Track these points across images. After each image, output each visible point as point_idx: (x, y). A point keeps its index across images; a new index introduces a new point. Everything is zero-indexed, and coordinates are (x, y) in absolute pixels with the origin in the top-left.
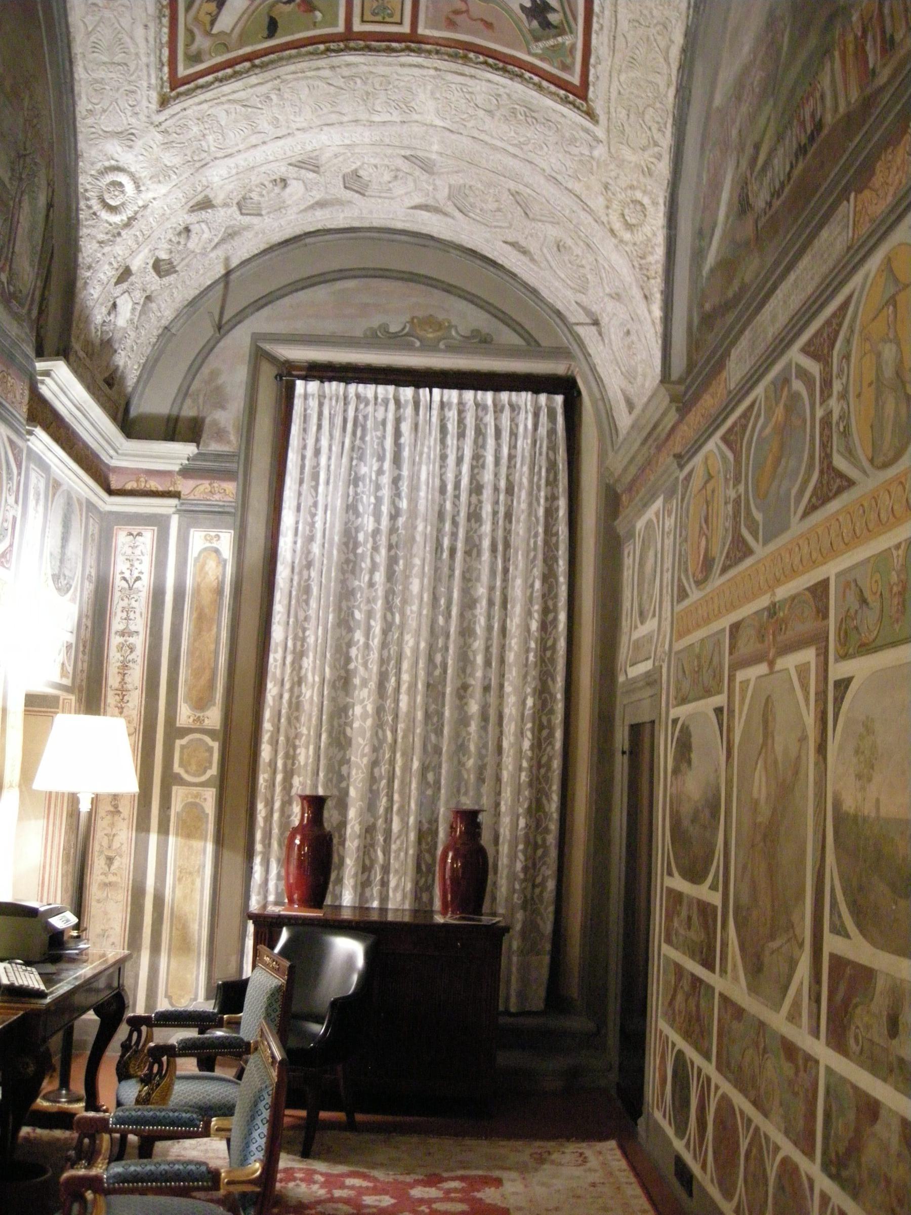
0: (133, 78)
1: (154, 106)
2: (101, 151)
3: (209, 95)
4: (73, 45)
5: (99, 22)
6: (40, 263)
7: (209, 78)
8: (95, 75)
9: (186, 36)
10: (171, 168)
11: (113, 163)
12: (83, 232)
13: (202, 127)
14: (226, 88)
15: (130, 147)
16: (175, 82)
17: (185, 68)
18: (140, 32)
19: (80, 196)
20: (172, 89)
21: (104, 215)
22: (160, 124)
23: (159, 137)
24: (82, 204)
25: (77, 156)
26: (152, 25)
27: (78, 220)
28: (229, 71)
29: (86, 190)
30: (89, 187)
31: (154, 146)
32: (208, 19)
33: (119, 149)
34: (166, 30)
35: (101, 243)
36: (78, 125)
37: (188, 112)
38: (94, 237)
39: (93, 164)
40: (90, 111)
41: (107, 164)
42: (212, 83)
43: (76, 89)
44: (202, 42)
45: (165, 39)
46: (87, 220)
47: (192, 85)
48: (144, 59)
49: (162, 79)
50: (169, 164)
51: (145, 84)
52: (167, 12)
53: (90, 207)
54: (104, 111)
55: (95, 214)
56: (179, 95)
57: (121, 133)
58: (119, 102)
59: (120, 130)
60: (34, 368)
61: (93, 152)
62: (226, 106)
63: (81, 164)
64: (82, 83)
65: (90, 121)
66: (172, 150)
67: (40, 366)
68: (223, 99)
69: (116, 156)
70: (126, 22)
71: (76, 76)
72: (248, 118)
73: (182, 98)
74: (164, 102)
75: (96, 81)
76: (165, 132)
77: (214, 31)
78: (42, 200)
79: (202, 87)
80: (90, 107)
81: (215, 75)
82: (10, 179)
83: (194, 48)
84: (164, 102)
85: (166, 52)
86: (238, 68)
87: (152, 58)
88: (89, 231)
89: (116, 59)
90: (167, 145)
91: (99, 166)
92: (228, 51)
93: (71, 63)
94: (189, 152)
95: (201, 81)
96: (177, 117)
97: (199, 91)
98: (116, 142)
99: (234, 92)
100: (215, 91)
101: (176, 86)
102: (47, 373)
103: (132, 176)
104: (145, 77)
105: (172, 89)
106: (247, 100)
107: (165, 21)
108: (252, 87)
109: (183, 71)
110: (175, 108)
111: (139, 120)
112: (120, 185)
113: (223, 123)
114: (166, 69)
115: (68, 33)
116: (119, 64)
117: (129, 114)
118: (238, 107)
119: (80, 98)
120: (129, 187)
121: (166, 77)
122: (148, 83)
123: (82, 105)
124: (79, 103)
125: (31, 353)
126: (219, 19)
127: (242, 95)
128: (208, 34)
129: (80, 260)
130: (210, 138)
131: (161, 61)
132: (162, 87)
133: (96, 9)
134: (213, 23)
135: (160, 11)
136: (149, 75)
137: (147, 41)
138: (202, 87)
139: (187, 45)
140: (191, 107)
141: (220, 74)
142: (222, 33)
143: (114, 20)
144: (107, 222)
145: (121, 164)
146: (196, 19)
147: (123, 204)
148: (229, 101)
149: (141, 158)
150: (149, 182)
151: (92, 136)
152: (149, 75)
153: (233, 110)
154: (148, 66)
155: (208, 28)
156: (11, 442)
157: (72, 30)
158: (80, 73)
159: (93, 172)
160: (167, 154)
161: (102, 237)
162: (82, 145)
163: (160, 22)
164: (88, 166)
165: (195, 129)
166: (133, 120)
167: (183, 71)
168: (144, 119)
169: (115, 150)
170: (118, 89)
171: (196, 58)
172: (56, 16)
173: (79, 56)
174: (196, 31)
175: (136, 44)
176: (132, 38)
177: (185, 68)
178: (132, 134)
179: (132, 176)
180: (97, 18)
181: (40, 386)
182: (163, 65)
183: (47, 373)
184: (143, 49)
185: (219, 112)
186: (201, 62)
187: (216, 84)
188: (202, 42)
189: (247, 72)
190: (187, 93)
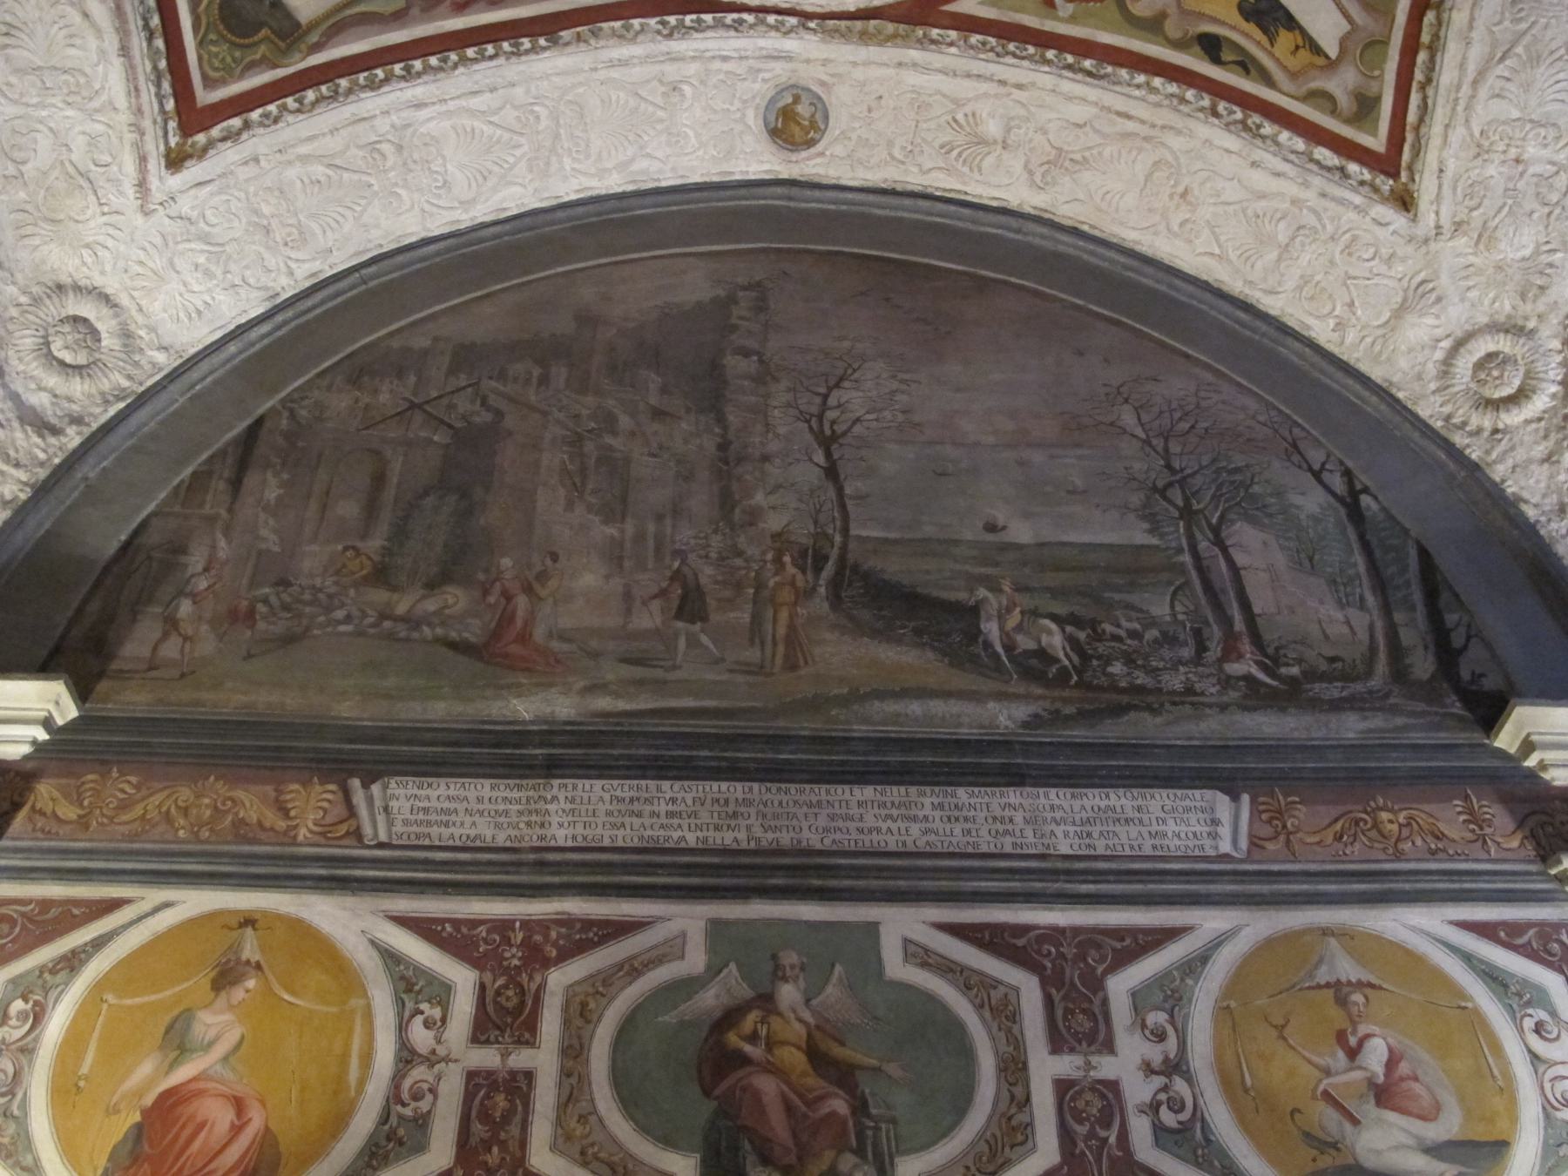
0: (1330, 228)
1: (1399, 220)
2: (1410, 350)
3: (1440, 115)
4: (1225, 288)
5: (1213, 233)
6: (1381, 585)
7: (1415, 99)
8: (1290, 284)
9: (1316, 107)
10: (1537, 252)
11: (1446, 344)
12: (1498, 472)
13: (1497, 158)
14: (1447, 76)
15: (1439, 300)
16: (1387, 163)
17: (1374, 133)
18: (1259, 179)
19: (1444, 432)
20: (1395, 175)
21: (1512, 418)
22: (1438, 227)
23: (1462, 242)
24: (1459, 439)
25: (1383, 393)
26: (1259, 154)
27: (1475, 468)
28: (1422, 57)
29: (1448, 418)
30: (1447, 409)
31: (1472, 259)
32: (1304, 55)
33: (1430, 321)
34: (1285, 136)
35: (1547, 459)
36: (1345, 358)
37: (1452, 166)
38: (1530, 461)
39: (1419, 377)
40: (1340, 326)
41: (1439, 355)
42: (1425, 99)
43: (1291, 323)
44: (1341, 84)
45: (1300, 144)
46: (1488, 452)
47: (1410, 137)
48: (1310, 196)
49: (1362, 183)
50: (1527, 252)
51: (1352, 215)
52: (1256, 118)
53: (1478, 432)
54: (1351, 304)
55: (1496, 431)
56: (1410, 168)
57: (1405, 300)
58: (1352, 272)
59: (1399, 300)
60: (1501, 754)
61: (1403, 363)
62: (1483, 92)
63: (1400, 395)
64: (1290, 310)
65: (1351, 336)
66: (1499, 234)
67: (1506, 739)
68: (1466, 90)
69: (1439, 332)
70: (1232, 192)
71: (1272, 312)
72: (1534, 60)
73: (1418, 166)
74: (1405, 201)
75: (1300, 288)
76: (1458, 226)
77: (1333, 52)
78: (1311, 501)
79: (1421, 120)
80: (1332, 323)
81: (1414, 85)
82: (1151, 531)
83: (1344, 101)
84: (1405, 201)
85: (1323, 154)
86: (1425, 38)
87: (1317, 181)
88: (1510, 462)
89: (1282, 238)
90: (1486, 237)
91: (1431, 369)
92: (1385, 43)
93: (1247, 307)
94: (1530, 204)
95: (1412, 117)
96: (1446, 190)
97: (1423, 130)
98: (1410, 318)
99: (1462, 66)
100: (1441, 101)
101: (1391, 168)
102: (1528, 747)
103: (1494, 328)
104: (1340, 209)
105: (1395, 175)
106: (1494, 45)
107: (1268, 129)
108: (1471, 27)
109: (1376, 142)
110: (1426, 188)
111: (1404, 260)
112: (1490, 356)
113: (1516, 114)
114: (1353, 168)
115: (1205, 286)
116: (1293, 239)
117: (1383, 269)
118: (1500, 70)
119: (1309, 328)
120: (1503, 344)
121: (1367, 175)
122: (1354, 211)
123: (1322, 332)
124: (1313, 334)
125: (1477, 737)
126: (1314, 35)
127: (1476, 53)
128: (1331, 65)
129: (1531, 513)
130: (1531, 150)
131: (1329, 169)
132: (1376, 190)
133: (1189, 226)
134: (1316, 49)
135: (1246, 128)
136: (1341, 202)
137: (1278, 175)
138: (1421, 120)
139: (1334, 111)
140: (1443, 158)
141: (1419, 76)
142: (1343, 43)
143: (1220, 209)
144: (1528, 422)
145: (1459, 334)
146: (1294, 75)
147: (1528, 375)
148: (1475, 83)
149: (1473, 294)
150: (1529, 307)
151: (1377, 348)
152: (1341, 202)
153: (1500, 83)
154: (1323, 195)
155: (1321, 61)
156: (1484, 930)
157: (1205, 277)
158: (1272, 305)
159: (1433, 386)
160: (1502, 246)
161: (1540, 450)
162: (1376, 373)
163: (1263, 138)
164: (1416, 386)
165: (1491, 170)
166: (1399, 269)
167: (1376, 142)
168: (1410, 249)
169: (1421, 329)
170: (1332, 262)
171: (1365, 107)
172: (1163, 288)
173: (1247, 291)
174: (1315, 85)
175: (1281, 194)
176: (1262, 196)
177: (1374, 133)
178: (1423, 282)
179: (1494, 328)
180: (1206, 232)
181: (1546, 776)
182: (1342, 169)
183: (1528, 747)
184: (1293, 190)
185: (1486, 110)
186: (1377, 99)
187: (1430, 92)
188: (1341, 84)
189: (1440, 24)
190: (1417, 151)
